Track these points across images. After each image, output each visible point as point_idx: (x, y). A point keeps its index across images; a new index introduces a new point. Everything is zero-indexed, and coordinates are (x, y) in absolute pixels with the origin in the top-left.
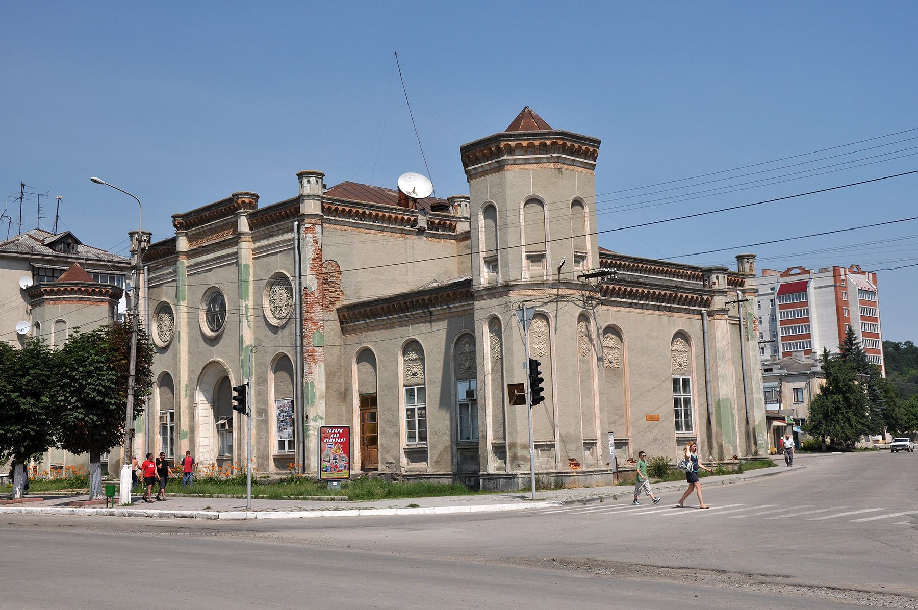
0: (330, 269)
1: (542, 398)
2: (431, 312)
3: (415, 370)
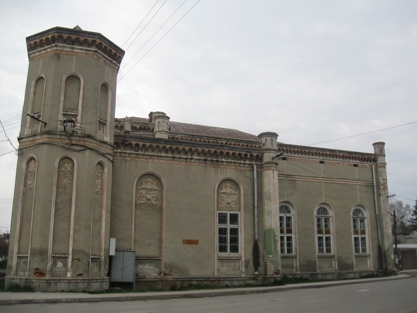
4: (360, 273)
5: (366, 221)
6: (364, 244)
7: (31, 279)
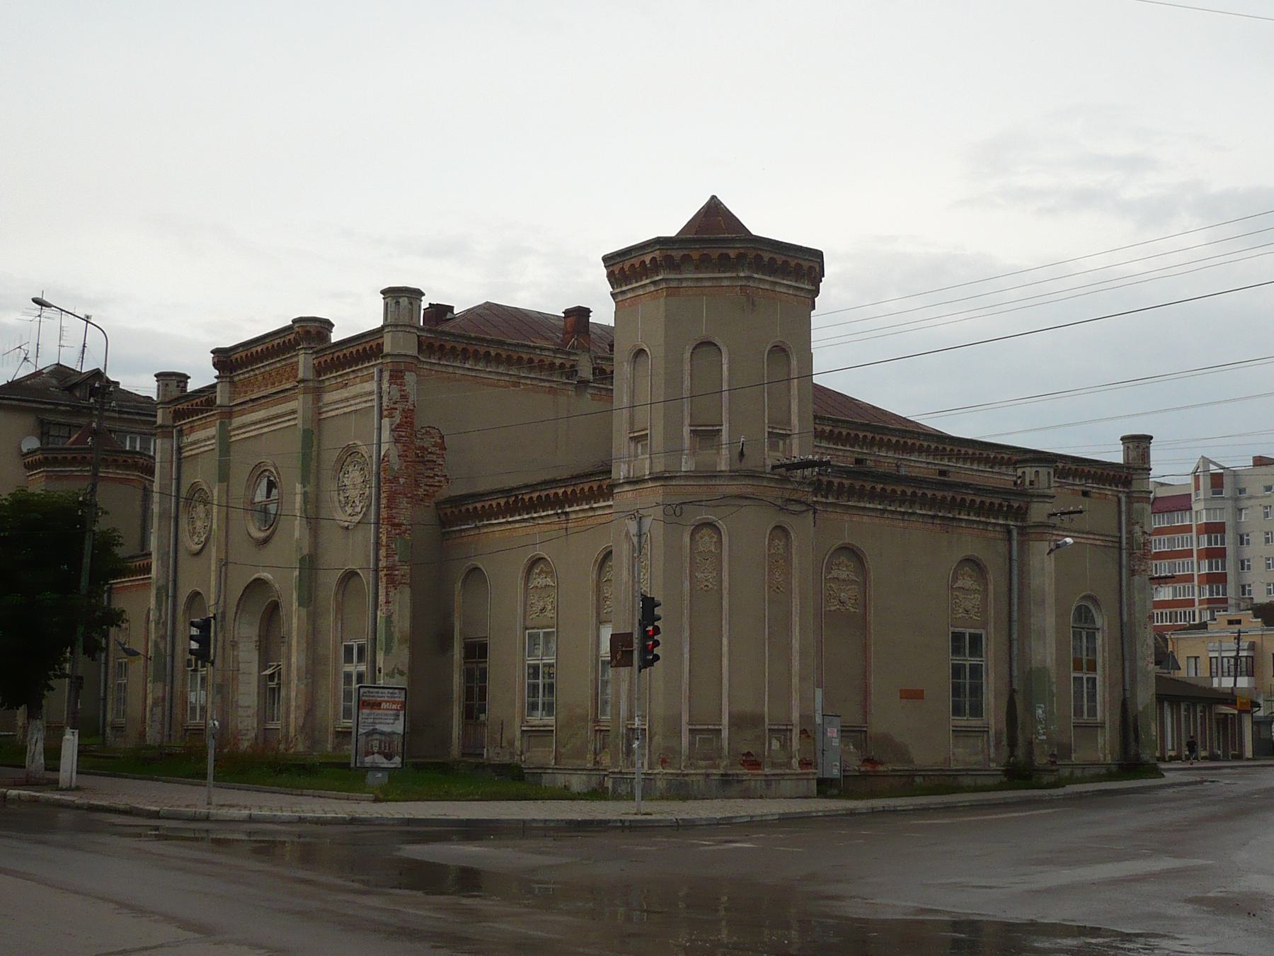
0: (427, 443)
1: (657, 658)
2: (567, 514)
4: (1084, 766)
5: (1099, 637)
6: (1092, 697)
7: (737, 775)
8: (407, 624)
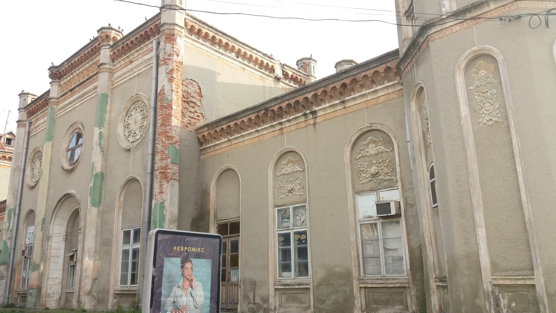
2: (314, 113)
3: (290, 186)
8: (176, 210)
